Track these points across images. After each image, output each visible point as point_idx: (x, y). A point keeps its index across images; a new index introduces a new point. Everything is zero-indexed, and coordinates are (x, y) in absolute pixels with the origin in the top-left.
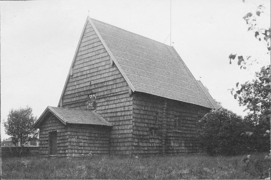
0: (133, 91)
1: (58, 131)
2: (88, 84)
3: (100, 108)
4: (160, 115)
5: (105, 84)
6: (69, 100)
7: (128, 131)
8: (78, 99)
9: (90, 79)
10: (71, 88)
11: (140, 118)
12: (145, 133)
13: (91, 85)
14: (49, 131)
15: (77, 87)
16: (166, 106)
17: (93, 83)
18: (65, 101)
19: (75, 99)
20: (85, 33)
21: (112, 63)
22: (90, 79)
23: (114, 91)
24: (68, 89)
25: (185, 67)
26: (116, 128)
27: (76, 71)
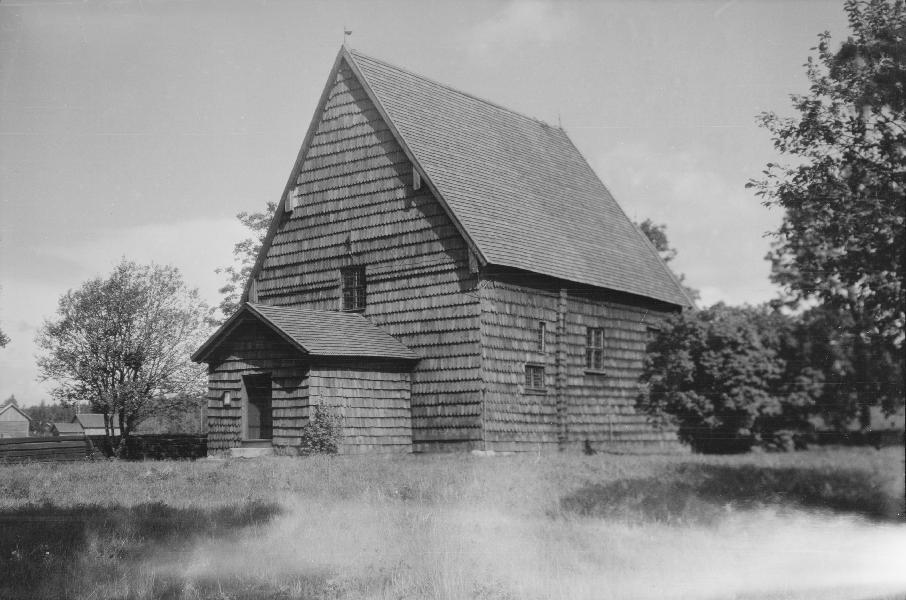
2: (342, 239)
3: (380, 308)
4: (550, 327)
6: (280, 283)
9: (346, 226)
11: (501, 337)
12: (514, 378)
13: (348, 244)
14: (246, 373)
15: (306, 245)
16: (564, 302)
17: (355, 236)
19: (297, 281)
20: (332, 94)
22: (346, 226)
25: (603, 190)
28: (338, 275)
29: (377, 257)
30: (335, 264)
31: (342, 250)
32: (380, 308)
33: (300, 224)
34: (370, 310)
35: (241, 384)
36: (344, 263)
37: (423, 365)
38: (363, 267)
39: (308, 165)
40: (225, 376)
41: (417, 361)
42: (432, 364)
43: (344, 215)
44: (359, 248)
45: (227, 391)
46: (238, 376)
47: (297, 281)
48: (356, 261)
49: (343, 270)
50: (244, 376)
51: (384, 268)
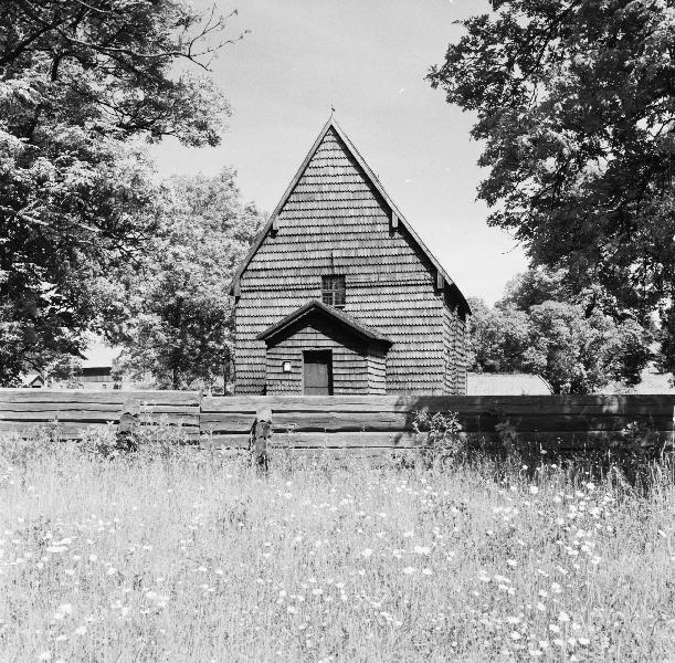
0: (450, 283)
1: (334, 351)
2: (327, 254)
3: (358, 307)
5: (371, 261)
6: (261, 282)
7: (433, 355)
8: (291, 281)
9: (327, 246)
10: (268, 257)
13: (332, 258)
14: (306, 349)
18: (245, 283)
19: (281, 281)
21: (395, 225)
22: (330, 246)
23: (398, 277)
24: (257, 258)
26: (403, 347)
27: (287, 223)
28: (320, 280)
29: (357, 270)
30: (316, 272)
31: (327, 263)
32: (358, 307)
33: (287, 240)
34: (348, 307)
35: (301, 357)
36: (326, 272)
37: (395, 347)
38: (343, 276)
39: (292, 198)
40: (282, 351)
41: (390, 344)
42: (403, 347)
43: (327, 238)
44: (341, 262)
45: (289, 361)
46: (296, 351)
47: (281, 281)
48: (337, 271)
49: (324, 277)
50: (305, 352)
51: (362, 278)
